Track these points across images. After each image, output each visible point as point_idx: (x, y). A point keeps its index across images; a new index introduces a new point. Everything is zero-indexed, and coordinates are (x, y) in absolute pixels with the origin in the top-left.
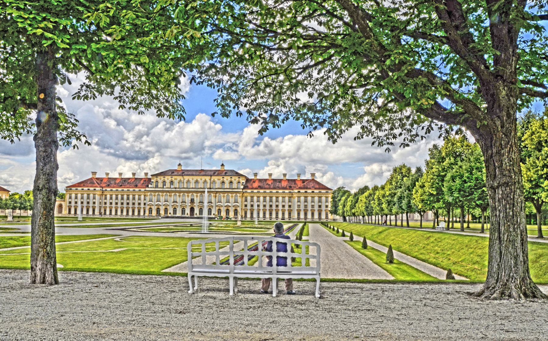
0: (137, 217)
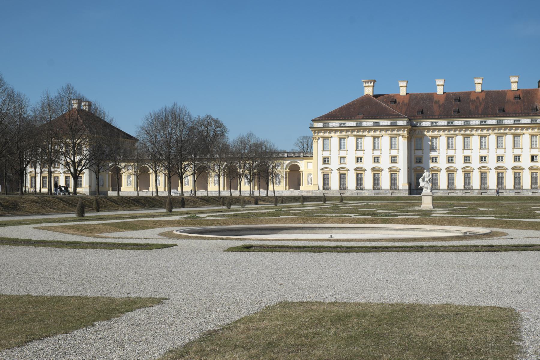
0: (512, 194)
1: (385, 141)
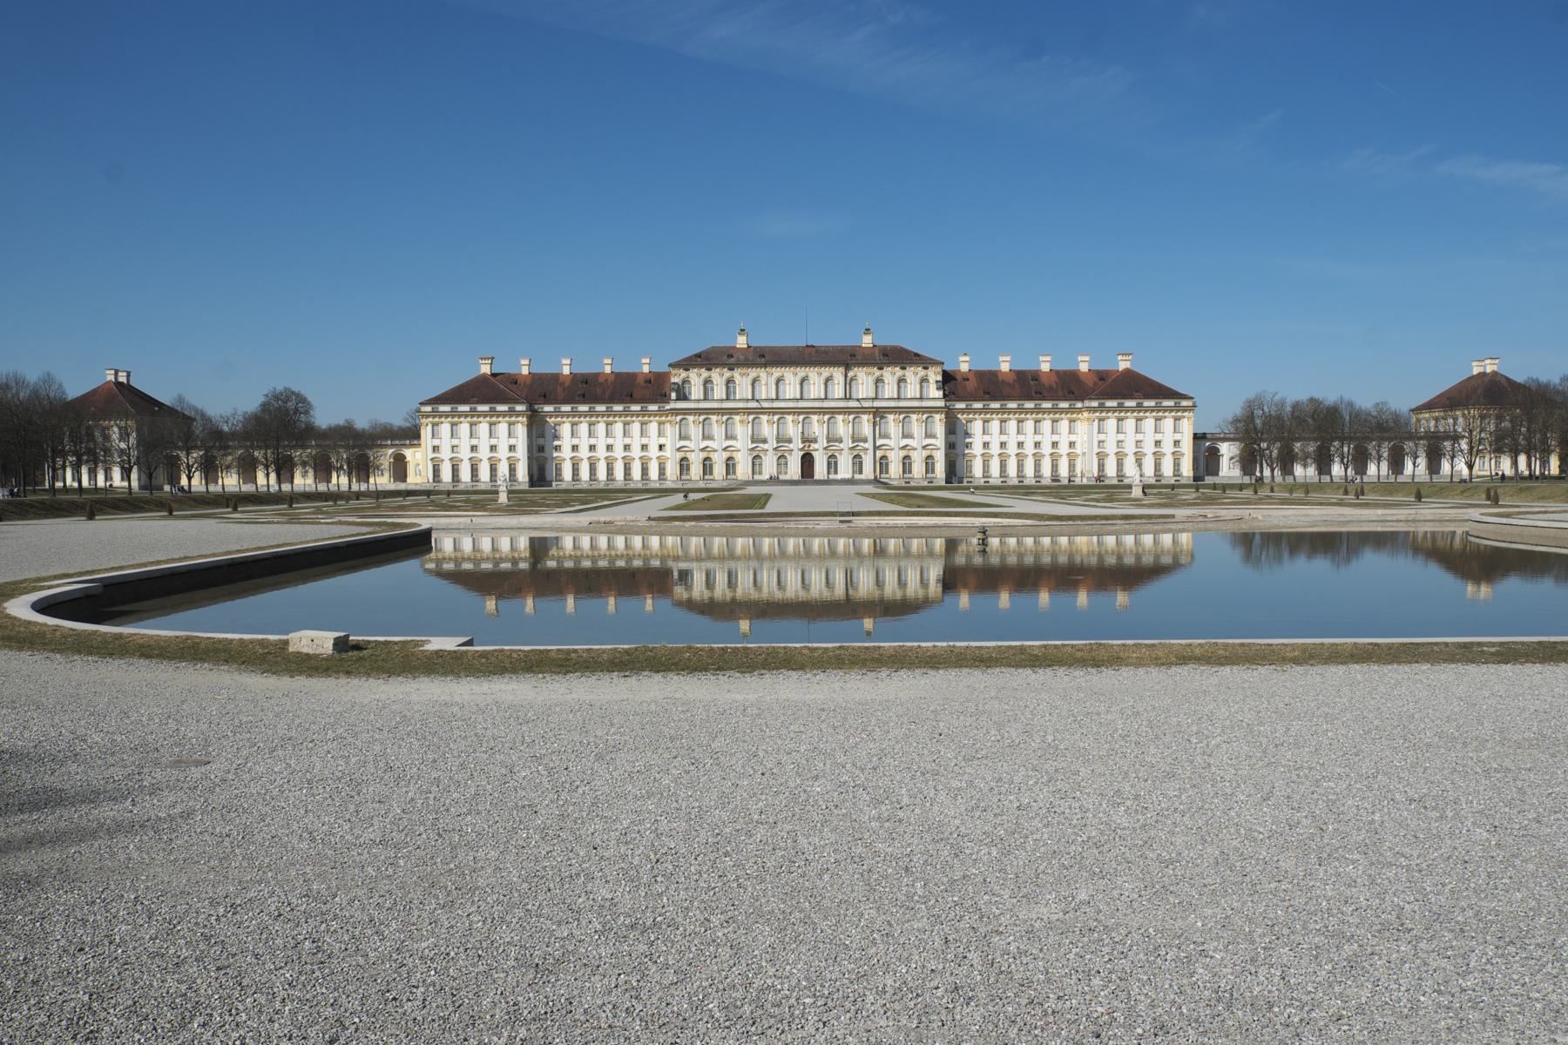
0: (640, 486)
1: (502, 428)
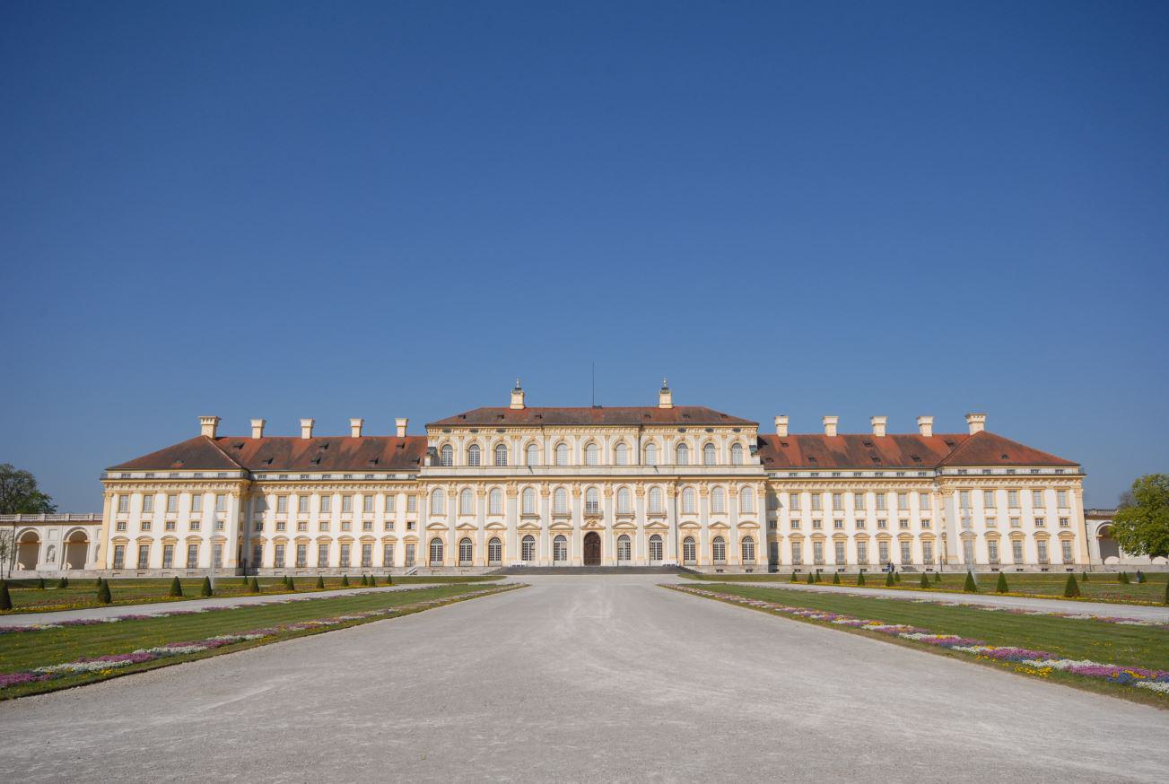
1: (208, 499)
